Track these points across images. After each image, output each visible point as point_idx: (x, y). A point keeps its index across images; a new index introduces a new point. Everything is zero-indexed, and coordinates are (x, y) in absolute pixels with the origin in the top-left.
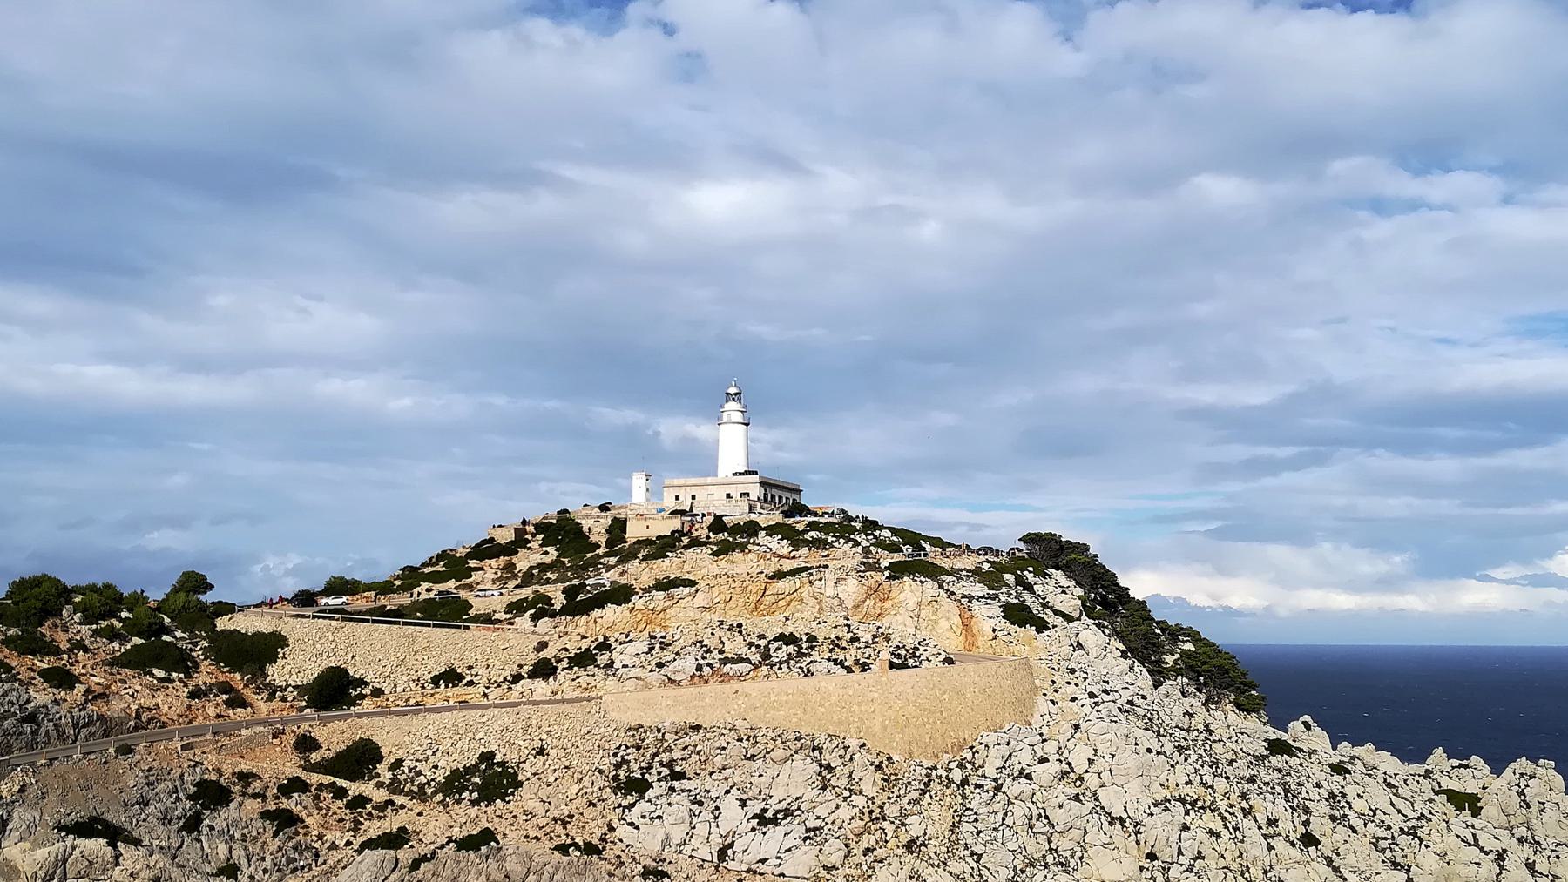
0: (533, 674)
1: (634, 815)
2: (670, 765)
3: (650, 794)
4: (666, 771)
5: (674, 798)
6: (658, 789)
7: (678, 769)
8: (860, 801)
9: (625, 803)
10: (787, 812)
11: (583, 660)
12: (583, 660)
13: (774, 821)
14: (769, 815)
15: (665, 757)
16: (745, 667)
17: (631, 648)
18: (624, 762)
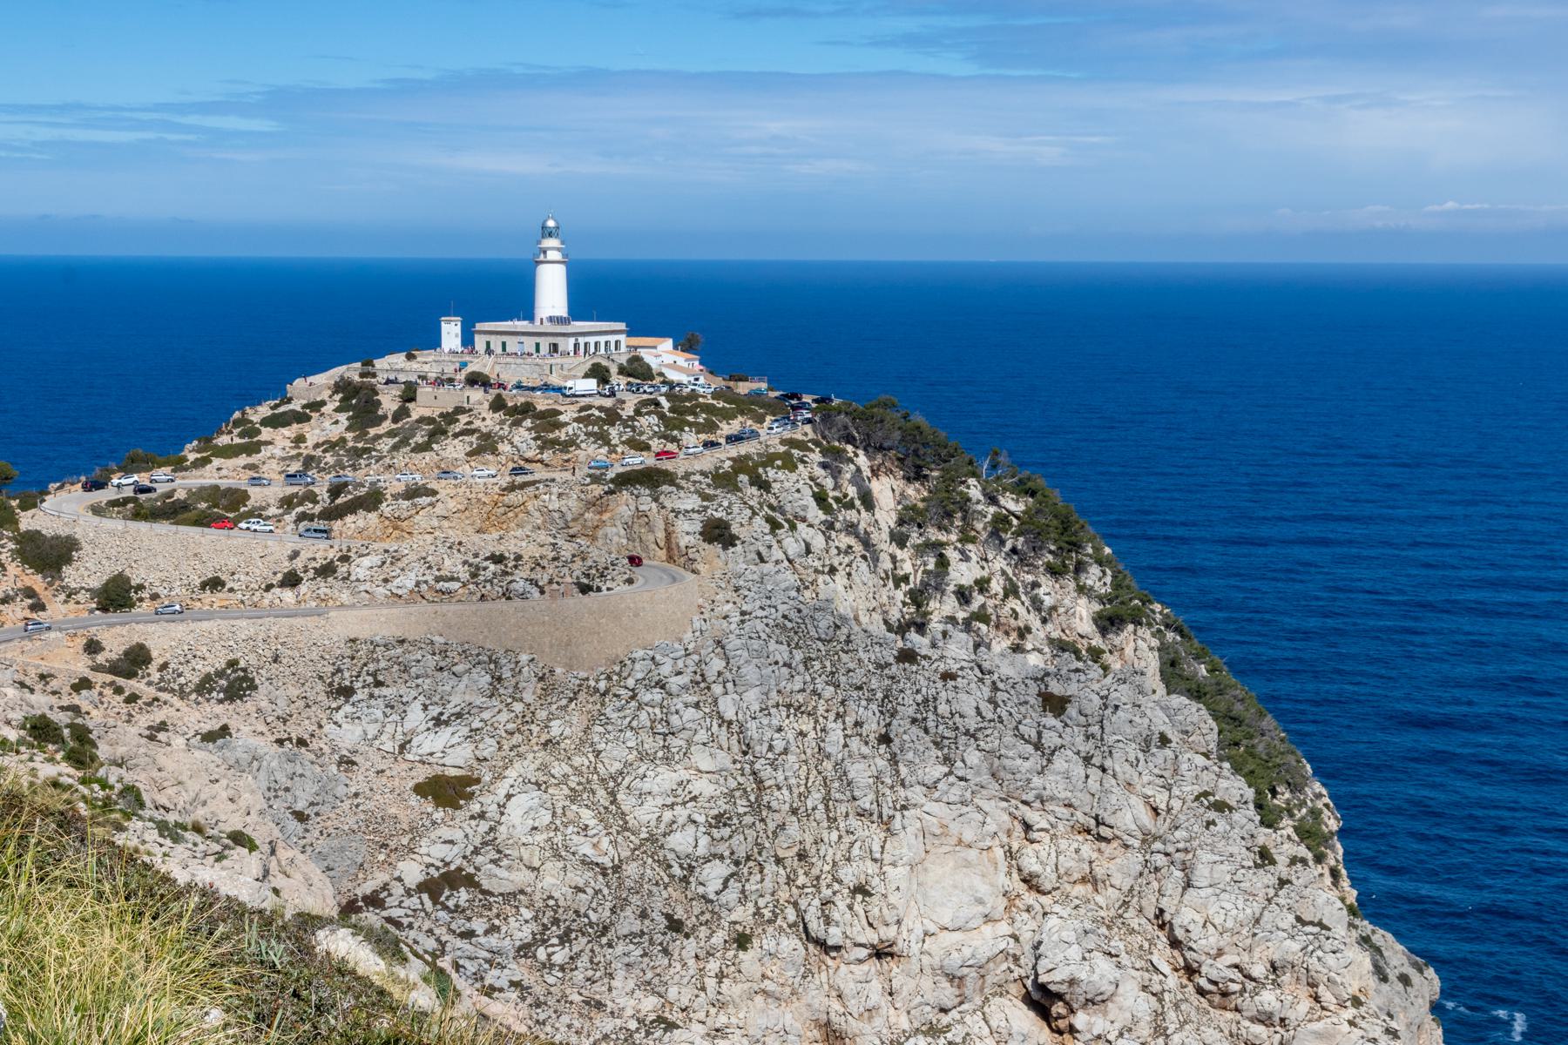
0: (282, 584)
1: (339, 716)
2: (374, 675)
3: (355, 698)
4: (370, 679)
5: (373, 702)
6: (361, 694)
7: (380, 678)
8: (518, 707)
9: (334, 705)
10: (459, 715)
11: (326, 571)
12: (326, 571)
13: (447, 723)
14: (444, 718)
15: (372, 667)
16: (455, 585)
17: (366, 562)
18: (339, 670)
